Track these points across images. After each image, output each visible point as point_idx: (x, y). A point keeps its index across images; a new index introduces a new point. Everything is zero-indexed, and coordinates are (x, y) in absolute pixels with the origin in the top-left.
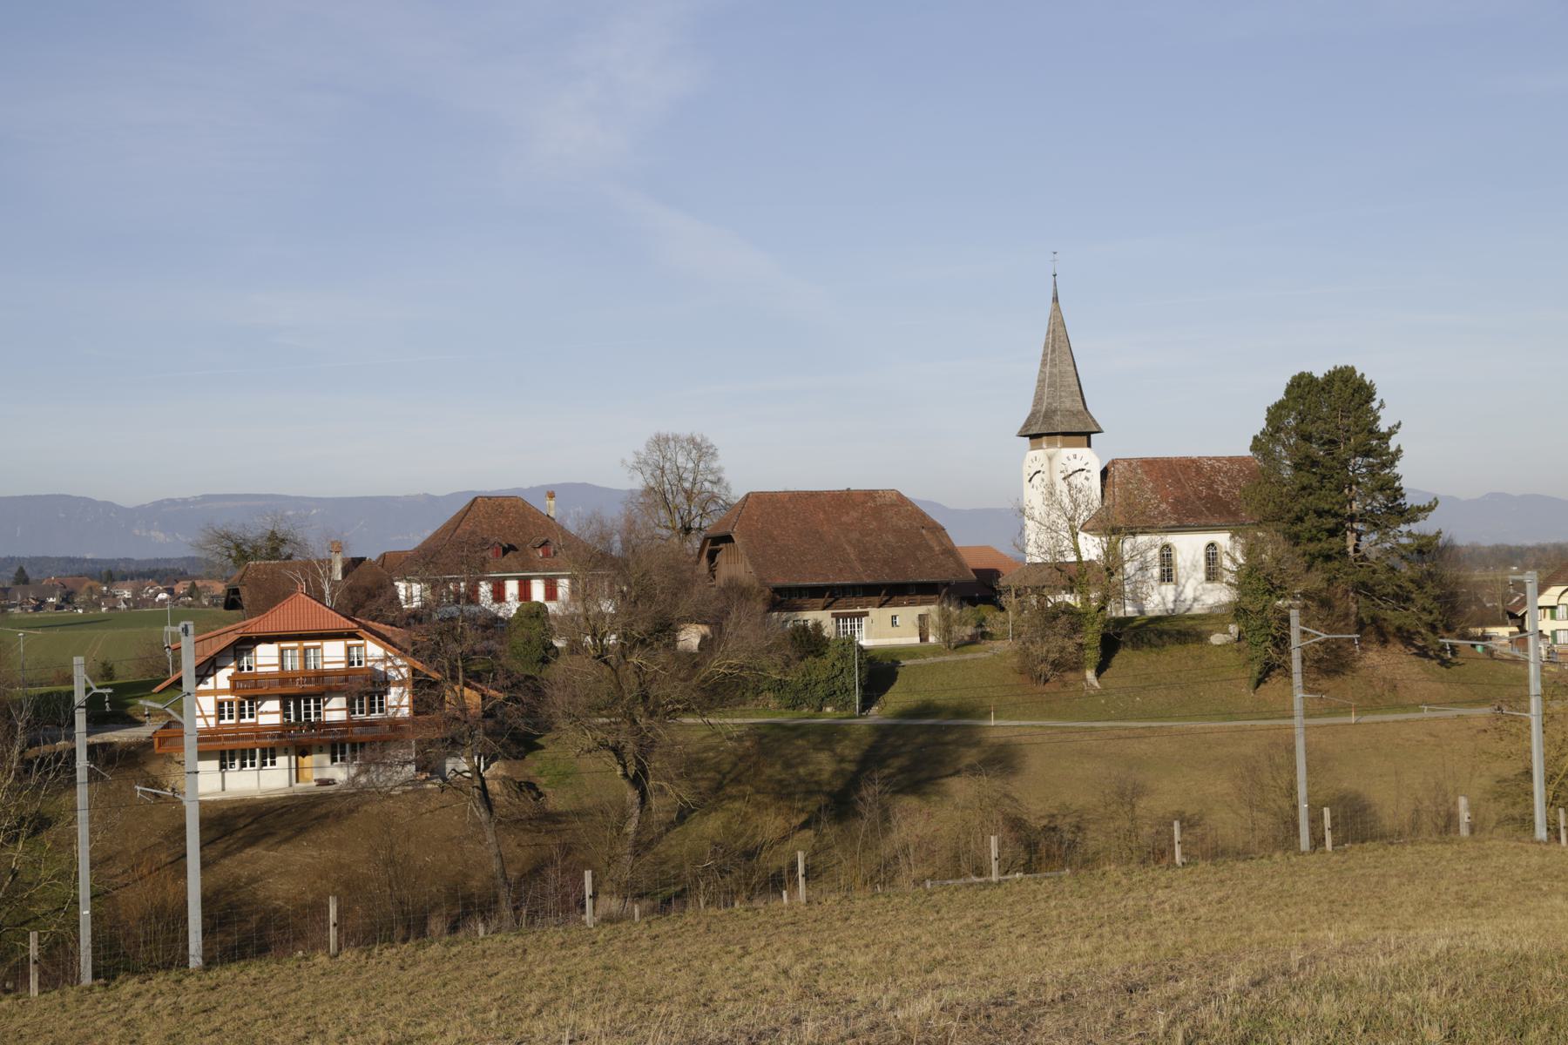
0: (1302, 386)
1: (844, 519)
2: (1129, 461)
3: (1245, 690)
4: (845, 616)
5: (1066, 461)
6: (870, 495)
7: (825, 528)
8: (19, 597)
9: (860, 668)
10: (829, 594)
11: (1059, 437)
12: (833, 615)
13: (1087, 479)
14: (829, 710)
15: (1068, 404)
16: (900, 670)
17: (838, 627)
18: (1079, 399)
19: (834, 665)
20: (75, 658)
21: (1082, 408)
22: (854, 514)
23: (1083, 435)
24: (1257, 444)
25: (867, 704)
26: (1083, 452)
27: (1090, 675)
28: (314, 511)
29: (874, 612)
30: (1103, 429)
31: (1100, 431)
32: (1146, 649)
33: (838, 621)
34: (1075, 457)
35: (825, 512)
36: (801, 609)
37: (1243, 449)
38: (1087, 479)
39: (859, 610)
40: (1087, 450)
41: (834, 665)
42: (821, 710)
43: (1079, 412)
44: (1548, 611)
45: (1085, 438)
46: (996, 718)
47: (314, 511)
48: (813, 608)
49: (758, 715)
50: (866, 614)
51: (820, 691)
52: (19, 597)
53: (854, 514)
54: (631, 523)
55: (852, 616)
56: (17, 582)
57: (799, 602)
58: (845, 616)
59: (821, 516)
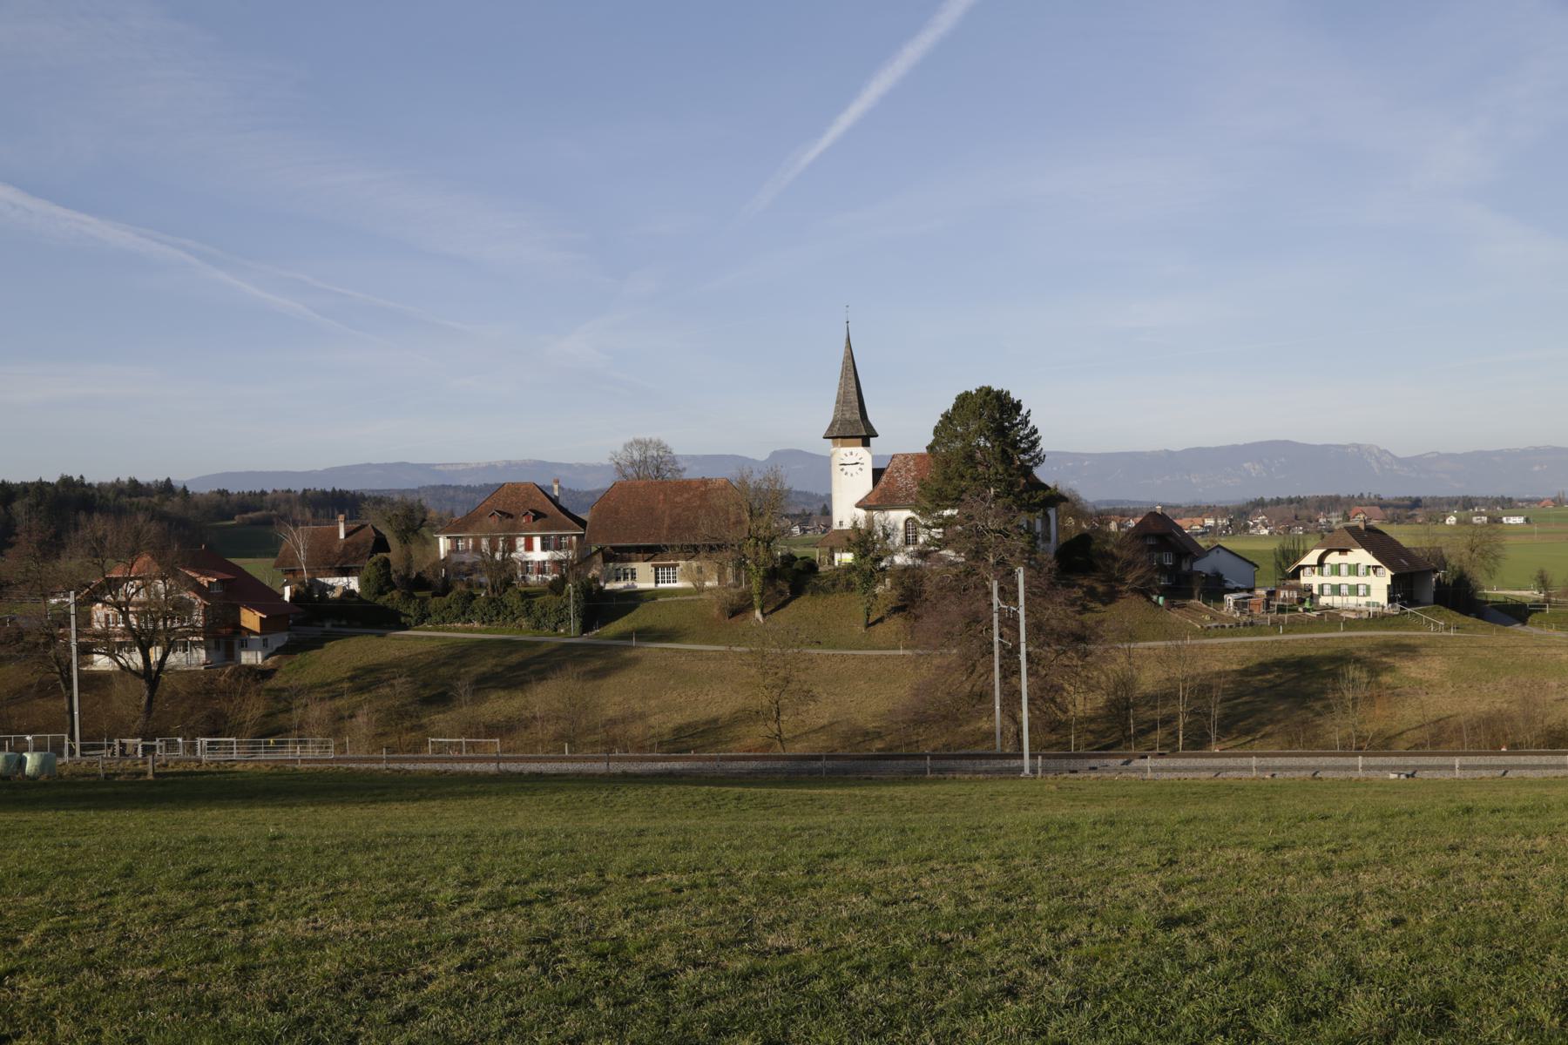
0: (963, 400)
1: (678, 499)
2: (906, 456)
3: (861, 629)
4: (663, 567)
5: (843, 457)
6: (704, 482)
7: (660, 505)
8: (815, 524)
9: (576, 602)
10: (650, 552)
11: (840, 440)
12: (652, 566)
13: (861, 469)
14: (562, 631)
15: (847, 416)
16: (643, 606)
17: (657, 574)
18: (858, 412)
19: (562, 601)
20: (356, 578)
21: (858, 417)
22: (686, 496)
23: (865, 436)
24: (930, 448)
25: (586, 627)
26: (859, 452)
27: (758, 613)
28: (1086, 463)
29: (682, 563)
30: (878, 433)
31: (877, 436)
32: (822, 595)
33: (657, 569)
34: (851, 454)
35: (665, 494)
36: (630, 560)
37: (925, 451)
38: (861, 469)
39: (672, 562)
40: (862, 448)
41: (562, 601)
42: (556, 630)
43: (856, 421)
44: (1317, 569)
45: (860, 440)
46: (1191, 639)
47: (1086, 463)
48: (637, 561)
49: (510, 632)
50: (678, 565)
51: (554, 619)
52: (815, 524)
53: (686, 496)
54: (789, 491)
55: (668, 567)
56: (822, 514)
57: (626, 554)
58: (663, 567)
59: (661, 497)
